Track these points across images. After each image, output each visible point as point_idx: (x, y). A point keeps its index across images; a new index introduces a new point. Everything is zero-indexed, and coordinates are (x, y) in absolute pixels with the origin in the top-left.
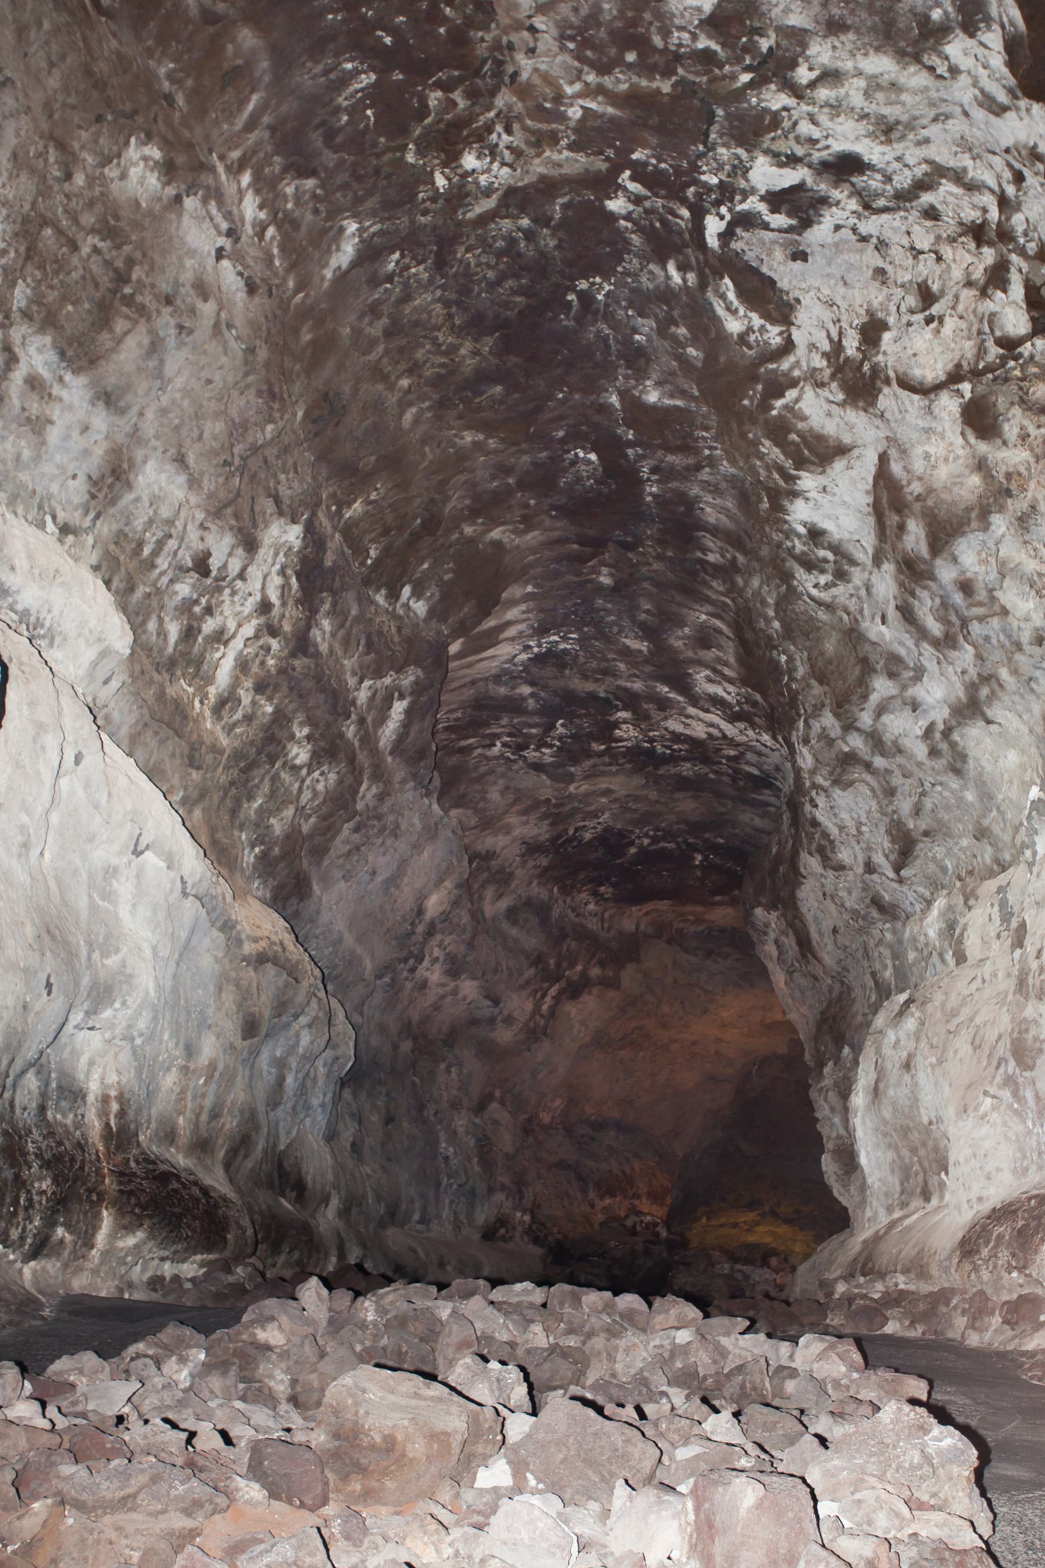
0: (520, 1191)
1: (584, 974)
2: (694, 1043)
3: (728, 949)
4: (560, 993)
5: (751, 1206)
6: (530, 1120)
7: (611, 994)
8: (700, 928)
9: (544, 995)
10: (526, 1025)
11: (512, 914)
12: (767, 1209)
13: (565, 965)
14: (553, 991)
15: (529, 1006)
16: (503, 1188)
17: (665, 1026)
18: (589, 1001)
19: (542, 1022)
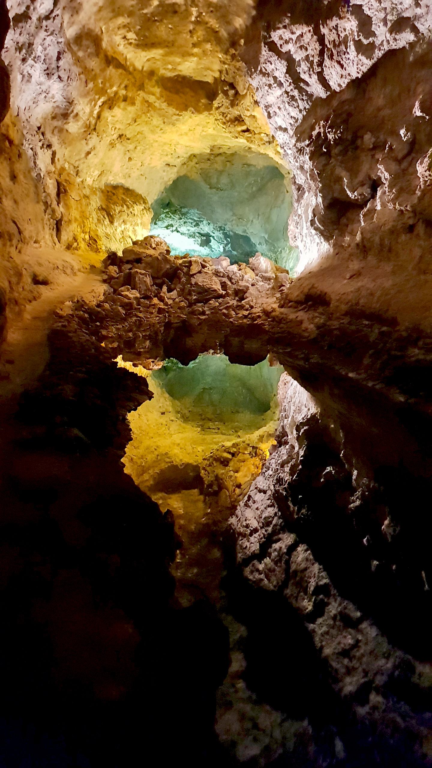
0: (83, 222)
1: (116, 93)
2: (165, 144)
3: (188, 90)
4: (104, 103)
5: (167, 227)
6: (82, 182)
7: (130, 109)
8: (174, 74)
9: (95, 105)
10: (85, 123)
11: (78, 39)
12: (174, 228)
13: (108, 85)
14: (100, 103)
15: (88, 110)
16: (76, 220)
17: (153, 132)
18: (117, 111)
19: (93, 122)
